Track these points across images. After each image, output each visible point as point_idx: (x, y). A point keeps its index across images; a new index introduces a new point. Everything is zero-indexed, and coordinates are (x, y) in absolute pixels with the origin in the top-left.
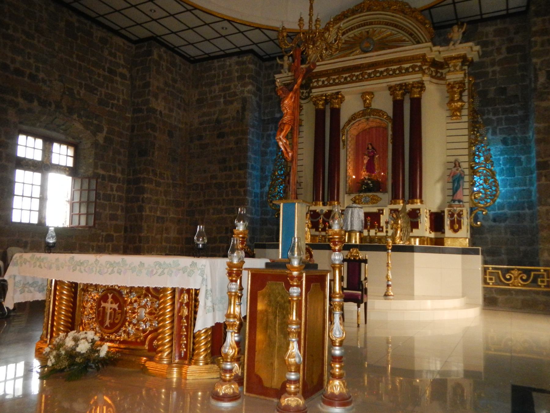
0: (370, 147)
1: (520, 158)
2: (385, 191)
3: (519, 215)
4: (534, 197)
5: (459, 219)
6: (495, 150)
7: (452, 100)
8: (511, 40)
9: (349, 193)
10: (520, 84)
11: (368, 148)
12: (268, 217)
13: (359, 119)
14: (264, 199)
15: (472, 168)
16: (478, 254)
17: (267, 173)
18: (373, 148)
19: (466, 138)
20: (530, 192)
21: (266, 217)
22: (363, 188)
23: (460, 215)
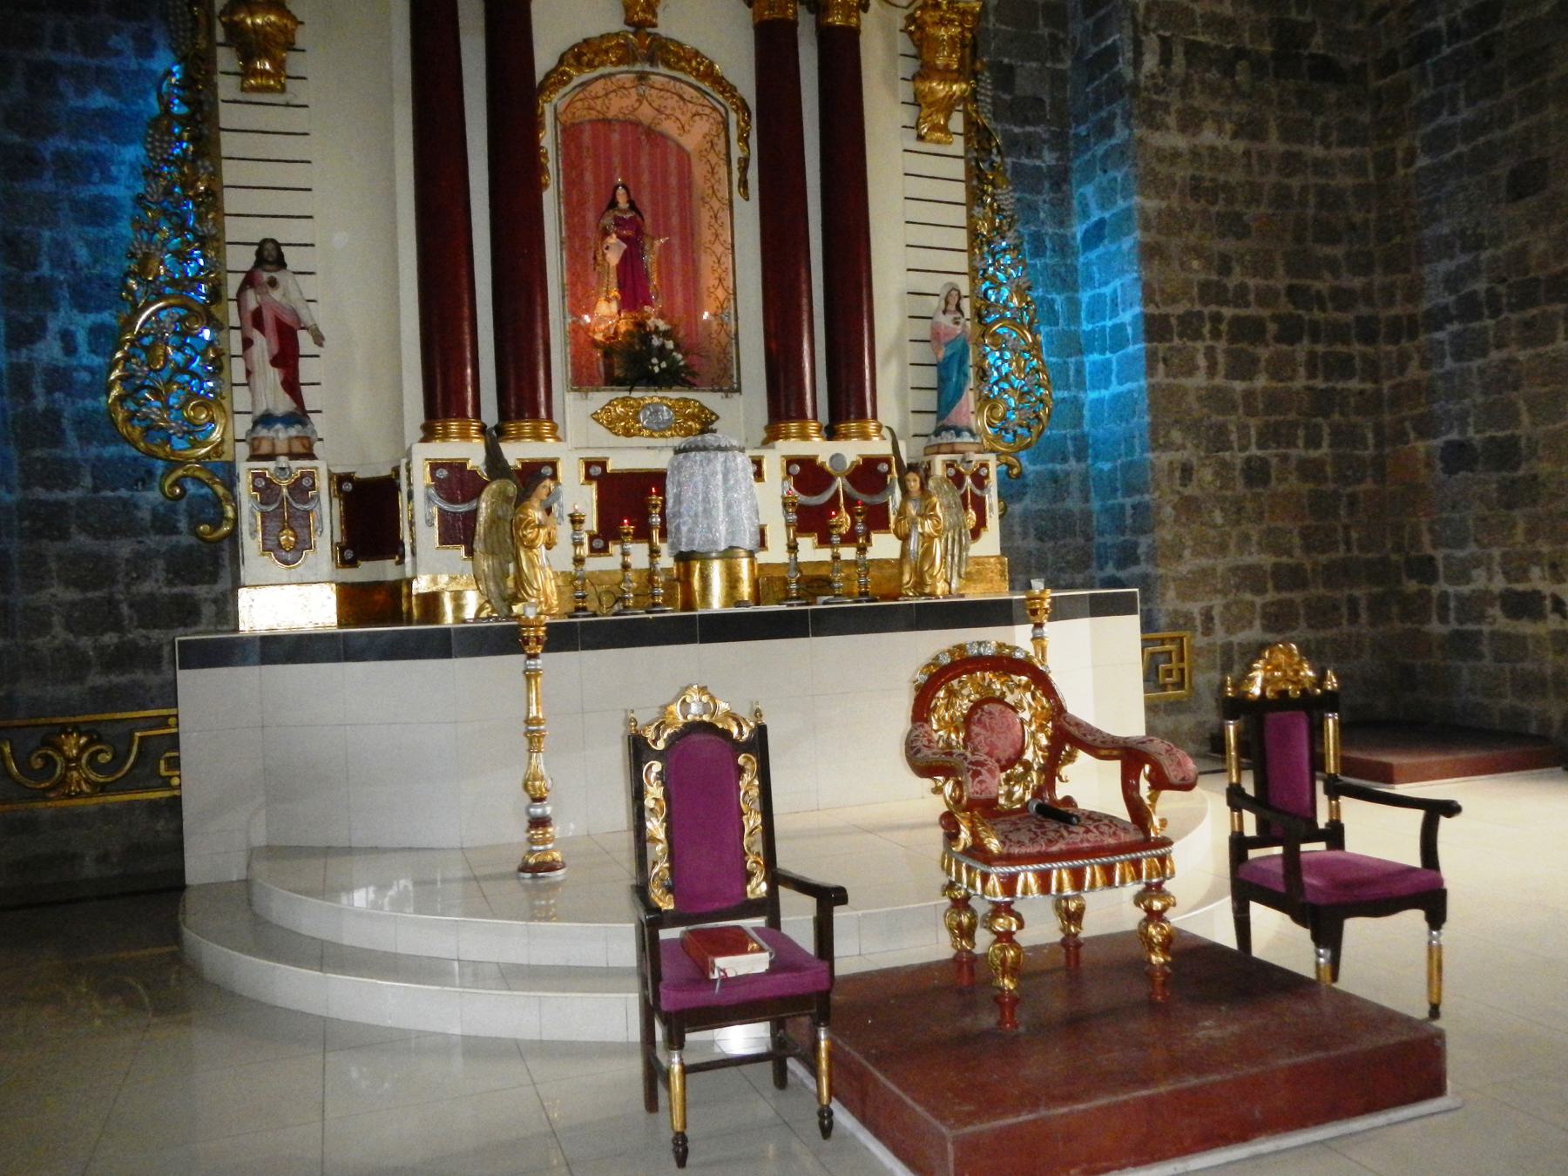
0: (622, 202)
1: (1053, 300)
2: (726, 382)
3: (1054, 478)
5: (978, 492)
7: (926, 71)
9: (582, 381)
10: (1048, 65)
11: (613, 204)
12: (74, 494)
13: (608, 69)
14: (40, 403)
15: (979, 316)
16: (1130, 610)
17: (45, 269)
18: (633, 206)
19: (959, 215)
20: (1077, 404)
21: (58, 495)
22: (656, 369)
23: (980, 480)
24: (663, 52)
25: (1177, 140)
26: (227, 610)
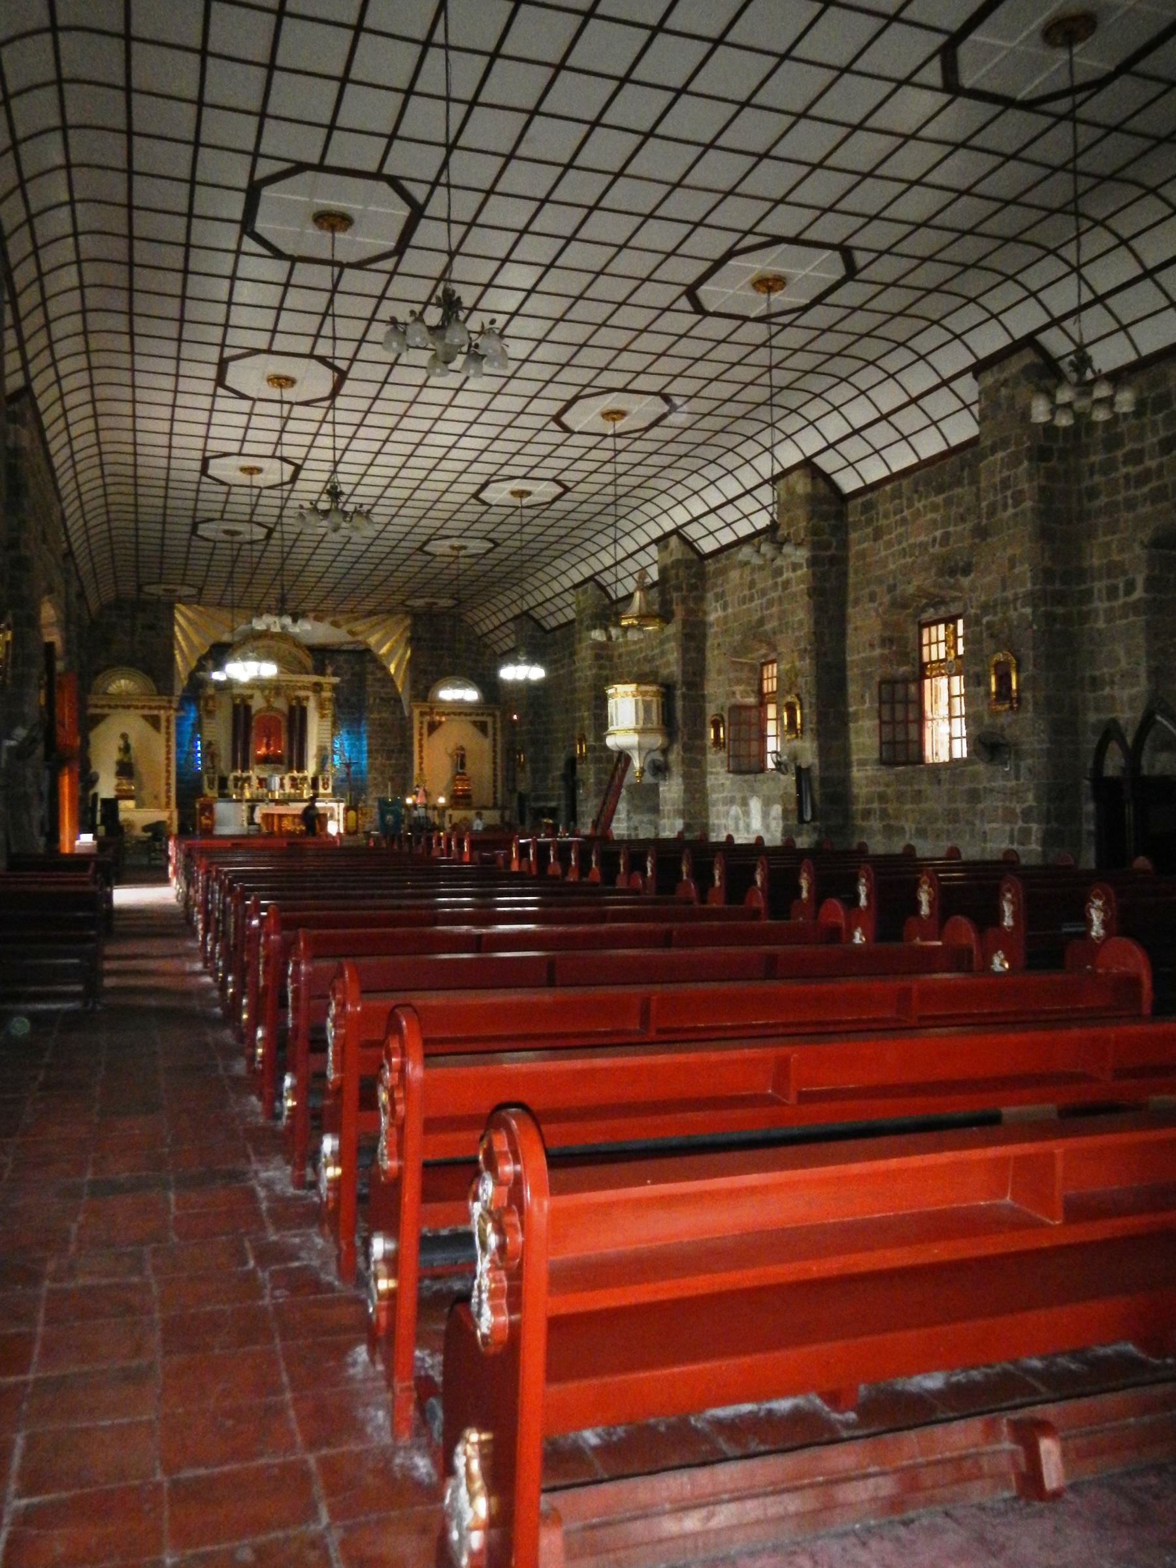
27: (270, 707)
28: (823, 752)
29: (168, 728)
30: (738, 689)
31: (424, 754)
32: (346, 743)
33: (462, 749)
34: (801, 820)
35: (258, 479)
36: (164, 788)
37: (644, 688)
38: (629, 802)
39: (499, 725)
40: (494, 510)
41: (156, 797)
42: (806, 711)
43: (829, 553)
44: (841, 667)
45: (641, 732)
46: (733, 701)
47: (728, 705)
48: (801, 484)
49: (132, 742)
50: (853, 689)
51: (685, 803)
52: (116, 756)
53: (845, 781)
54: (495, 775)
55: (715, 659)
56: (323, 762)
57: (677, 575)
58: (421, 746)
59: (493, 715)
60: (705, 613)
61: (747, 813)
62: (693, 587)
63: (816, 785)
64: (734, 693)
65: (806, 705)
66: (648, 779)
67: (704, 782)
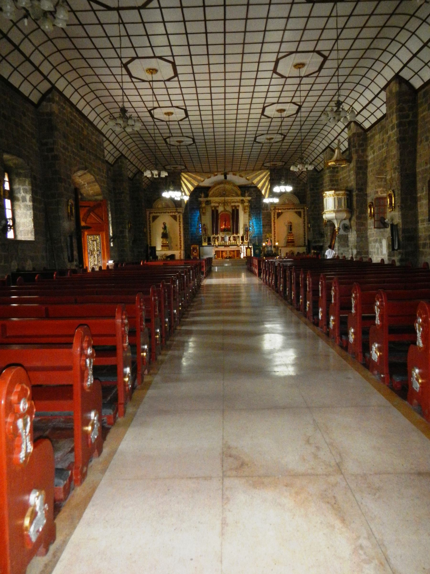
2: (230, 231)
4: (262, 233)
6: (254, 220)
8: (257, 193)
24: (227, 211)
25: (265, 211)
26: (202, 244)
27: (225, 210)
28: (404, 216)
29: (179, 219)
30: (379, 190)
31: (276, 225)
32: (254, 223)
33: (291, 223)
34: (393, 249)
35: (172, 118)
36: (179, 242)
37: (338, 192)
38: (339, 243)
39: (306, 213)
40: (274, 120)
41: (177, 246)
42: (396, 197)
43: (407, 120)
44: (414, 175)
45: (336, 212)
46: (377, 196)
47: (375, 197)
48: (394, 87)
49: (167, 226)
50: (419, 185)
51: (357, 243)
52: (160, 231)
53: (416, 230)
54: (305, 233)
55: (371, 177)
56: (246, 230)
57: (354, 140)
58: (274, 222)
59: (304, 209)
60: (367, 156)
61: (381, 246)
62: (361, 145)
63: (400, 233)
64: (377, 192)
65: (396, 194)
66: (342, 232)
67: (367, 233)
